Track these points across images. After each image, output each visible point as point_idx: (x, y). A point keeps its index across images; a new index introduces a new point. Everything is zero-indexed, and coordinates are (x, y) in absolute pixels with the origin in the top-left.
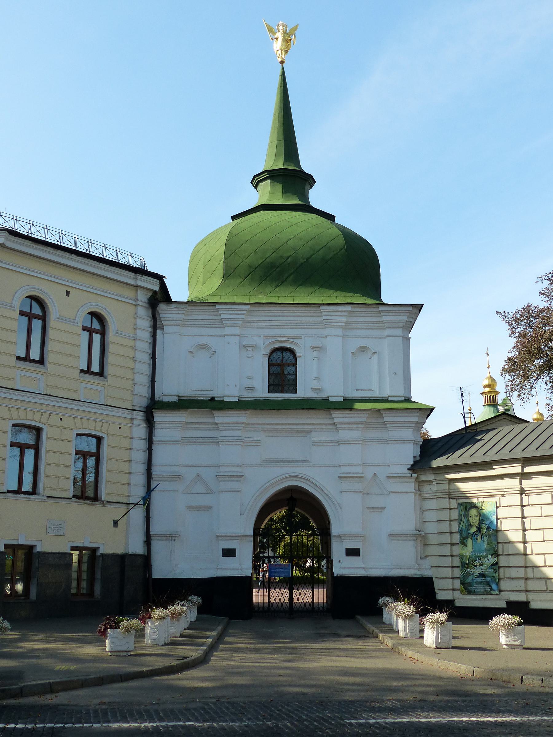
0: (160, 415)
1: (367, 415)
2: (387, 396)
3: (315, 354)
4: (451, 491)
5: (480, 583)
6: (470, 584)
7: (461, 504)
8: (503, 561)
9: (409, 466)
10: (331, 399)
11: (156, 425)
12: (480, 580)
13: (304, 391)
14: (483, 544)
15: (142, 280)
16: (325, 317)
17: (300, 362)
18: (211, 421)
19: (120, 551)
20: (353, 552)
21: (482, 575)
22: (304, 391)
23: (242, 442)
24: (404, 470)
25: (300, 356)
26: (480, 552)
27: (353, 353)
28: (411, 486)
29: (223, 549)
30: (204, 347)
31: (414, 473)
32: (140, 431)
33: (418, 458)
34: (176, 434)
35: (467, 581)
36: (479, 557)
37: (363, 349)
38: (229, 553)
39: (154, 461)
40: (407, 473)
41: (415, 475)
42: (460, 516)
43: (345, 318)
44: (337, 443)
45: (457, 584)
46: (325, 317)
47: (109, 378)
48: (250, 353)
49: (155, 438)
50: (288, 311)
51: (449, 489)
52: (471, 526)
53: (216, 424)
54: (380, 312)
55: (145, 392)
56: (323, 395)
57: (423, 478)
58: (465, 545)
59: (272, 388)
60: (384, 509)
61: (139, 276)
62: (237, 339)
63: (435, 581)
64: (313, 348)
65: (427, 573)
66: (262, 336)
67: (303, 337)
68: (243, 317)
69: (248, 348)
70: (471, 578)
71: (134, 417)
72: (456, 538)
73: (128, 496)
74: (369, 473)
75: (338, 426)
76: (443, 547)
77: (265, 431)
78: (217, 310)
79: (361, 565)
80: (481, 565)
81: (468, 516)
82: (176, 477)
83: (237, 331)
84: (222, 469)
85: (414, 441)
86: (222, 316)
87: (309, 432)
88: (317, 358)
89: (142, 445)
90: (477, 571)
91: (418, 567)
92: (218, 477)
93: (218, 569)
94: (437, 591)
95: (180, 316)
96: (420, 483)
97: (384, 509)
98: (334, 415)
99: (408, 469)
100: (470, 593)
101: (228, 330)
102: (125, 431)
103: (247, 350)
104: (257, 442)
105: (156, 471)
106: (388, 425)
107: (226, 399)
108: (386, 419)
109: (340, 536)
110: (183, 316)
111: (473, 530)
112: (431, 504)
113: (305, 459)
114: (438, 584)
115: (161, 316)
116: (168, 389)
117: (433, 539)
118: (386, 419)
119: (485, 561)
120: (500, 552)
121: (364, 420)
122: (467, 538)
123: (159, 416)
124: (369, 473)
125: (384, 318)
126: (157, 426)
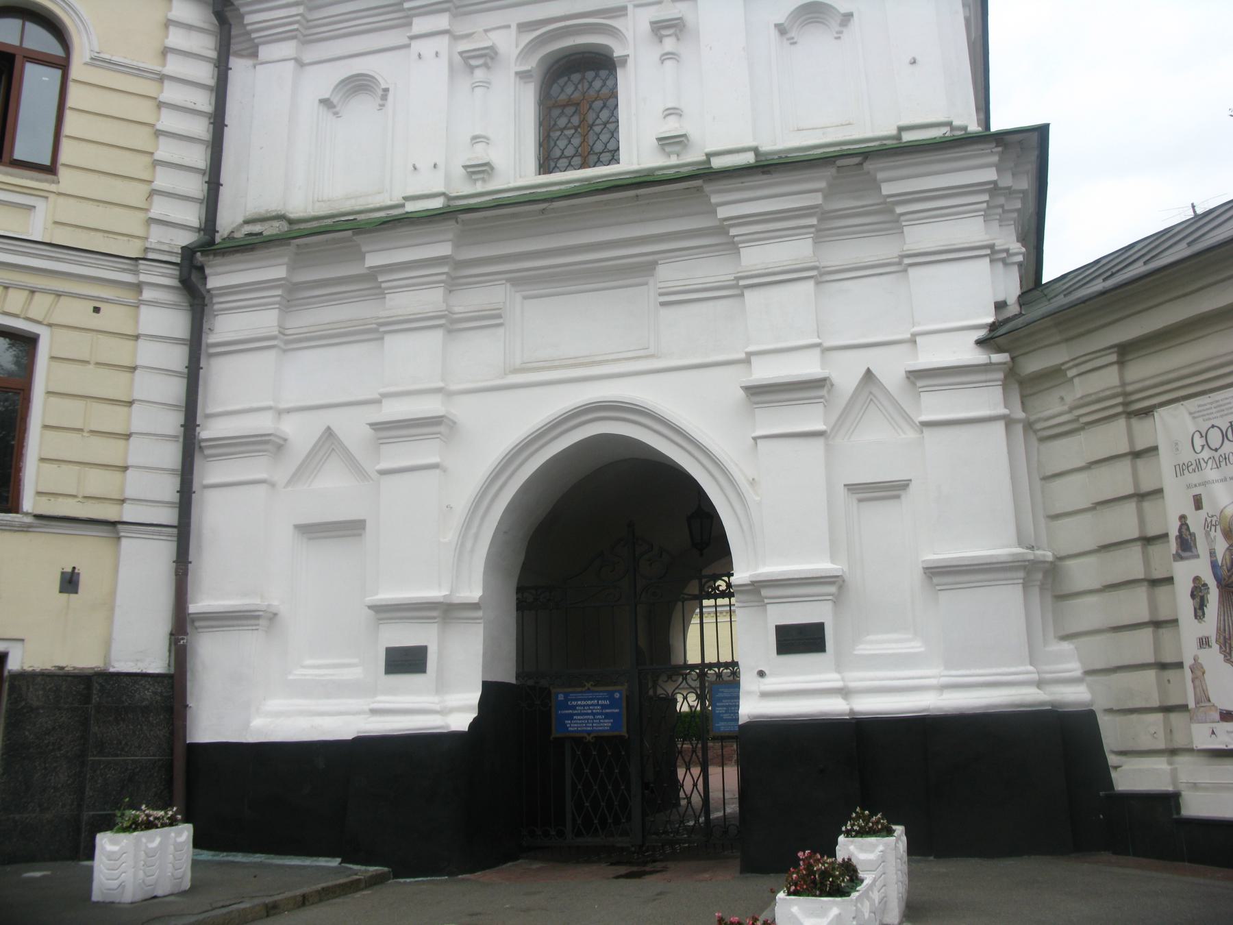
0: (220, 269)
1: (822, 184)
2: (894, 132)
3: (669, 44)
4: (1129, 389)
9: (982, 333)
11: (215, 300)
13: (638, 151)
19: (81, 657)
22: (638, 151)
23: (451, 324)
24: (965, 352)
27: (782, 30)
28: (988, 400)
31: (1000, 350)
32: (165, 319)
33: (1013, 309)
34: (265, 320)
40: (978, 357)
44: (738, 288)
47: (62, 172)
48: (479, 74)
51: (1123, 384)
53: (372, 275)
55: (192, 216)
56: (693, 156)
57: (1033, 364)
59: (546, 164)
60: (903, 485)
62: (442, 43)
63: (1104, 721)
66: (514, 27)
67: (630, 8)
69: (473, 62)
71: (143, 278)
74: (845, 374)
75: (733, 232)
76: (1122, 594)
77: (518, 281)
79: (832, 679)
85: (991, 247)
87: (646, 268)
88: (667, 56)
91: (1035, 677)
92: (377, 426)
94: (1112, 759)
97: (903, 485)
98: (714, 199)
99: (980, 343)
102: (113, 317)
103: (472, 69)
104: (491, 319)
106: (899, 210)
108: (887, 189)
113: (641, 353)
114: (1111, 733)
115: (248, 19)
117: (1083, 574)
118: (887, 189)
123: (219, 277)
124: (845, 374)
126: (218, 303)
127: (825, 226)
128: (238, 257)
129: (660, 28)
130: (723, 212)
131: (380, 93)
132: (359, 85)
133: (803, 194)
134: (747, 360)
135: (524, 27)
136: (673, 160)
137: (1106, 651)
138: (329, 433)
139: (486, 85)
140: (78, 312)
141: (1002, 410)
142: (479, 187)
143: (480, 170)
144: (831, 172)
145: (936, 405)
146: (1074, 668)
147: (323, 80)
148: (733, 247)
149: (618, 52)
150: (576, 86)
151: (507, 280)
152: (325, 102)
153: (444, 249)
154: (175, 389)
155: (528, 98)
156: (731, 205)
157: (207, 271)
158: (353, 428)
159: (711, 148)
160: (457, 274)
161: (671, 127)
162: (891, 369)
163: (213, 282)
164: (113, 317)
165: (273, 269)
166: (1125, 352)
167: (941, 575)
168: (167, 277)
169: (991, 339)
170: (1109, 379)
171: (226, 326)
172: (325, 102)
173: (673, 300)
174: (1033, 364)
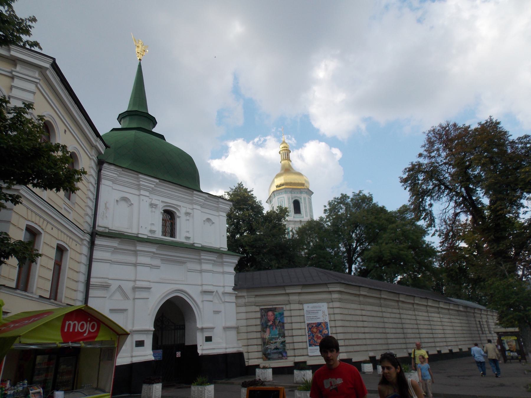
3: (188, 218)
5: (275, 353)
6: (269, 354)
7: (262, 309)
8: (288, 340)
10: (196, 245)
12: (275, 351)
13: (180, 238)
14: (276, 331)
15: (99, 144)
16: (195, 198)
17: (178, 221)
18: (132, 248)
20: (209, 339)
21: (276, 348)
22: (180, 238)
23: (151, 266)
24: (230, 290)
25: (179, 217)
26: (275, 335)
28: (233, 299)
29: (136, 341)
30: (125, 199)
32: (85, 250)
35: (267, 352)
36: (275, 338)
37: (208, 220)
38: (140, 344)
39: (93, 274)
41: (236, 292)
42: (262, 316)
43: (203, 201)
44: (201, 271)
45: (260, 355)
46: (195, 198)
48: (154, 209)
49: (94, 257)
50: (179, 190)
52: (269, 321)
54: (218, 202)
55: (90, 221)
56: (191, 242)
57: (240, 294)
58: (265, 332)
59: (164, 233)
61: (99, 139)
64: (187, 214)
65: (241, 350)
68: (153, 186)
70: (269, 350)
72: (259, 328)
73: (74, 300)
78: (138, 178)
80: (276, 343)
81: (267, 315)
82: (106, 287)
83: (147, 194)
84: (138, 283)
86: (141, 183)
87: (184, 263)
89: (84, 260)
90: (273, 346)
93: (132, 357)
94: (246, 360)
95: (115, 175)
96: (237, 297)
99: (233, 289)
100: (269, 359)
101: (142, 192)
104: (158, 267)
105: (93, 281)
107: (140, 236)
108: (224, 260)
109: (202, 329)
110: (116, 176)
111: (270, 323)
112: (243, 309)
114: (246, 356)
116: (105, 222)
119: (278, 340)
120: (286, 335)
121: (215, 259)
122: (266, 328)
123: (98, 241)
125: (220, 205)
126: (95, 248)
127: (214, 263)
128: (107, 238)
129: (187, 214)
130: (202, 257)
131: (130, 203)
132: (125, 199)
133: (213, 257)
134: (202, 285)
135: (162, 202)
136: (187, 242)
137: (245, 342)
138: (120, 286)
139: (154, 212)
140: (73, 244)
141: (235, 301)
142: (153, 235)
143: (152, 232)
144: (218, 255)
145: (228, 299)
146: (241, 345)
147: (118, 195)
148: (200, 263)
149: (178, 214)
150: (170, 217)
151: (162, 260)
152: (117, 201)
153: (154, 250)
154: (83, 269)
155: (161, 217)
156: (205, 256)
157: (96, 239)
158: (127, 286)
159: (195, 242)
160: (154, 255)
161: (188, 235)
162: (221, 290)
163: (97, 242)
164: (78, 248)
165: (114, 243)
166: (256, 296)
167: (226, 329)
168: (88, 238)
169: (234, 289)
170: (252, 299)
171: (97, 254)
172: (117, 201)
173: (190, 271)
174: (240, 294)
